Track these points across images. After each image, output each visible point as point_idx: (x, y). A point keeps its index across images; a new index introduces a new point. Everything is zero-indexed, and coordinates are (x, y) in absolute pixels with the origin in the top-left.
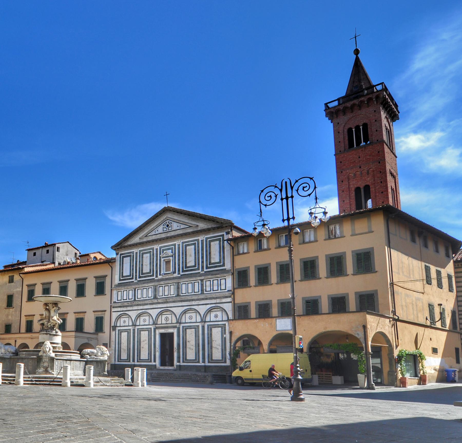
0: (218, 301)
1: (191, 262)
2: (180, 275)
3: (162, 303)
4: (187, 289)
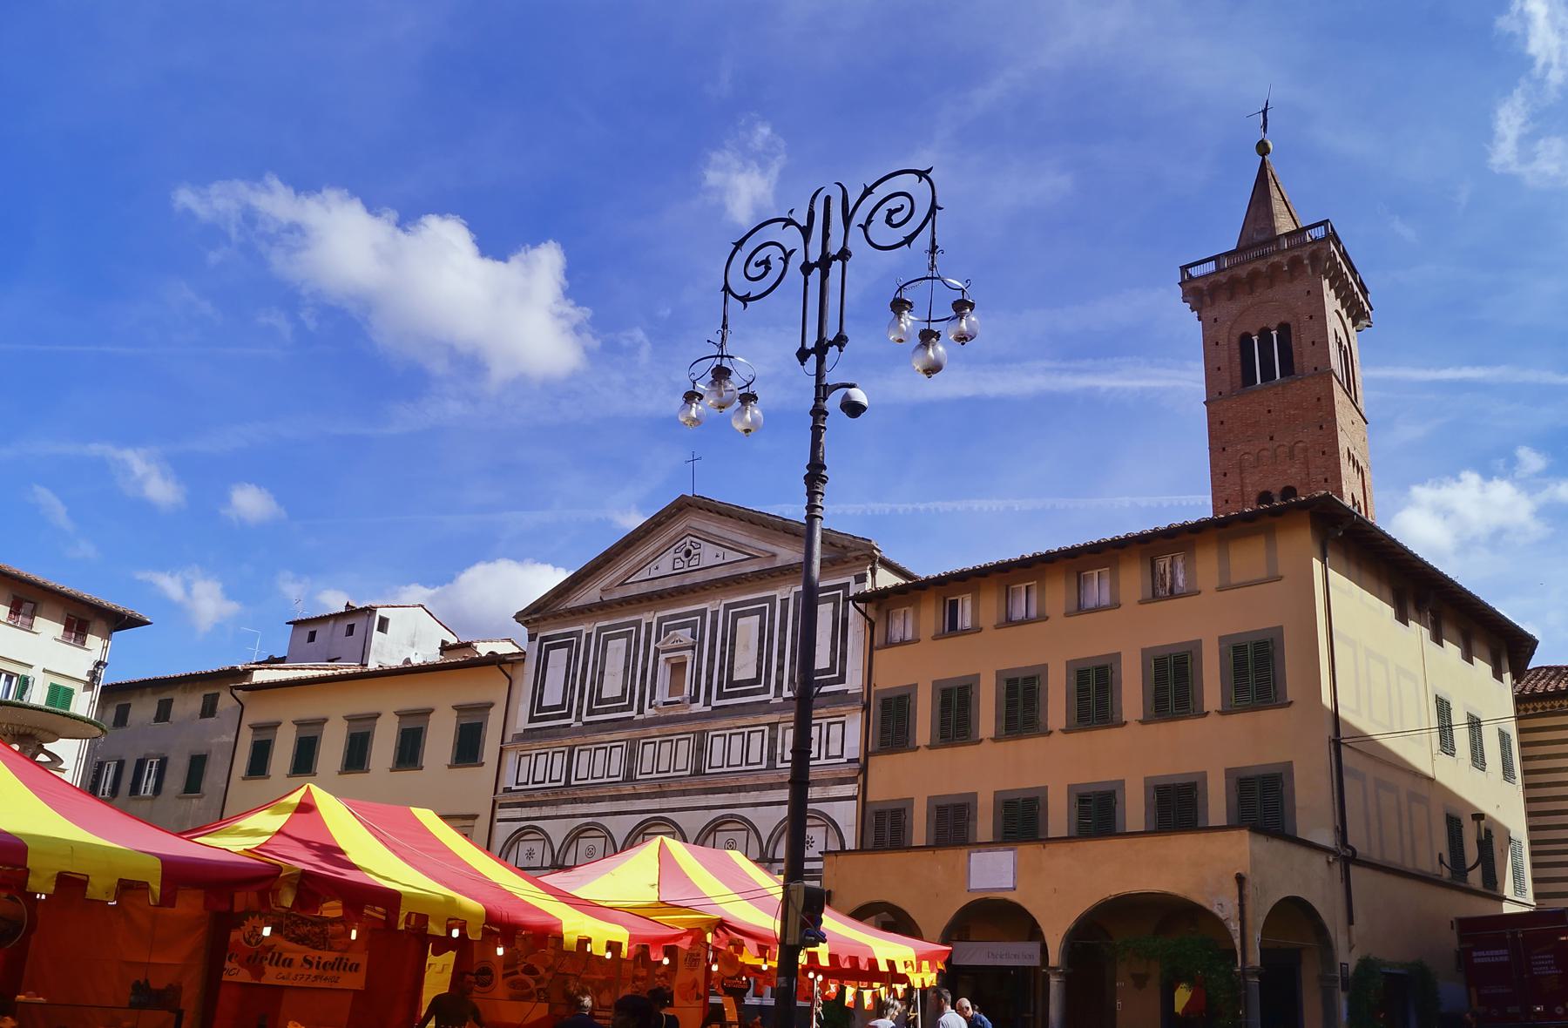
1: (745, 668)
2: (709, 709)
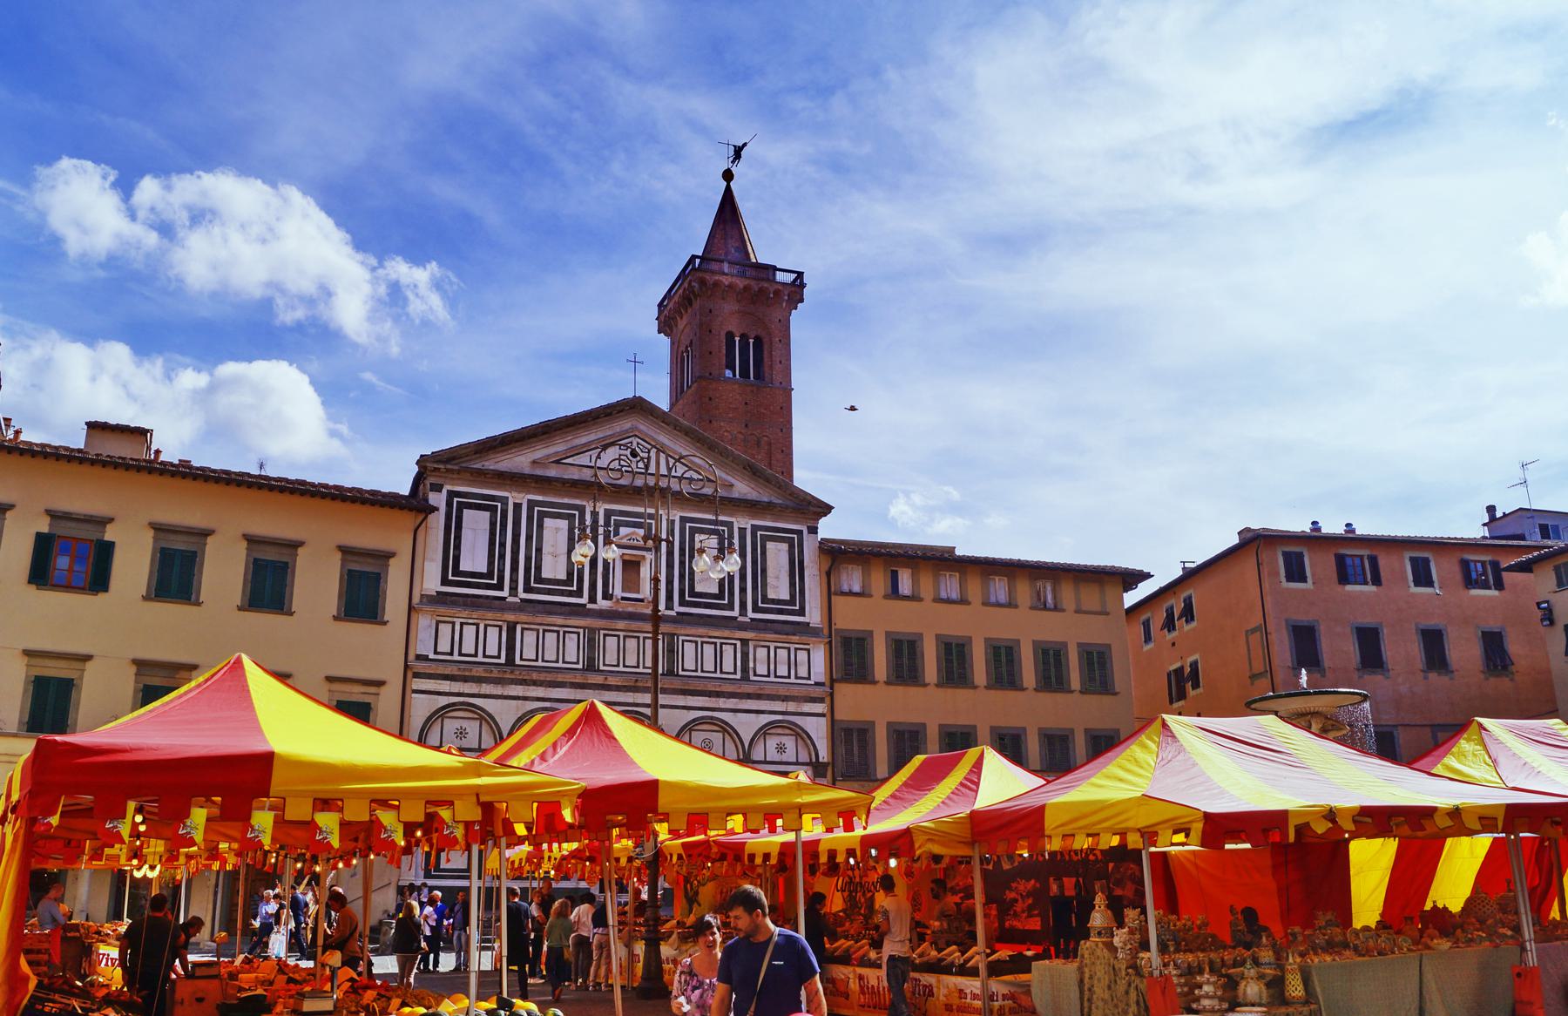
0: (791, 706)
3: (618, 688)
4: (699, 657)
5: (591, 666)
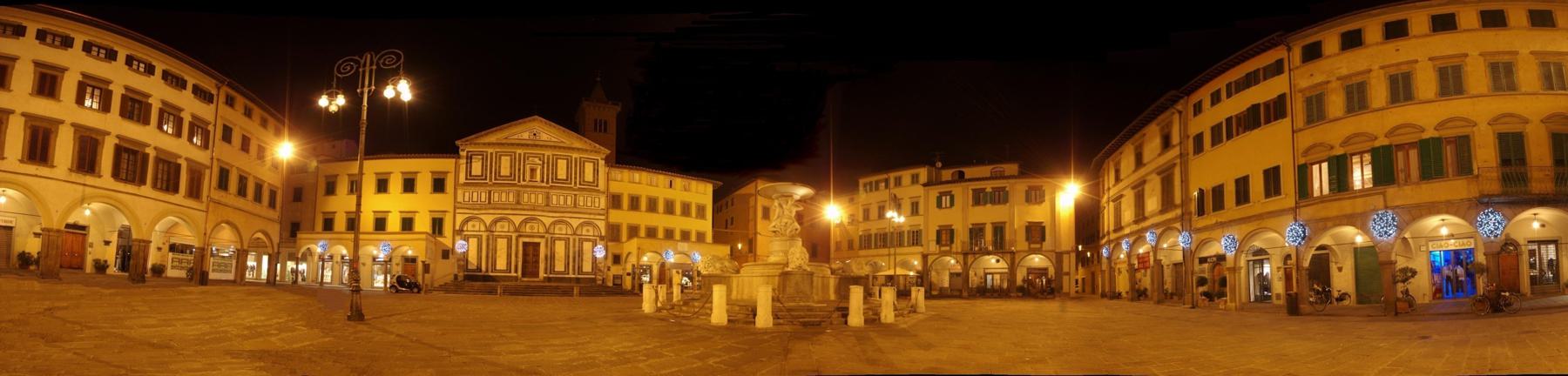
1: (562, 174)
5: (518, 203)
